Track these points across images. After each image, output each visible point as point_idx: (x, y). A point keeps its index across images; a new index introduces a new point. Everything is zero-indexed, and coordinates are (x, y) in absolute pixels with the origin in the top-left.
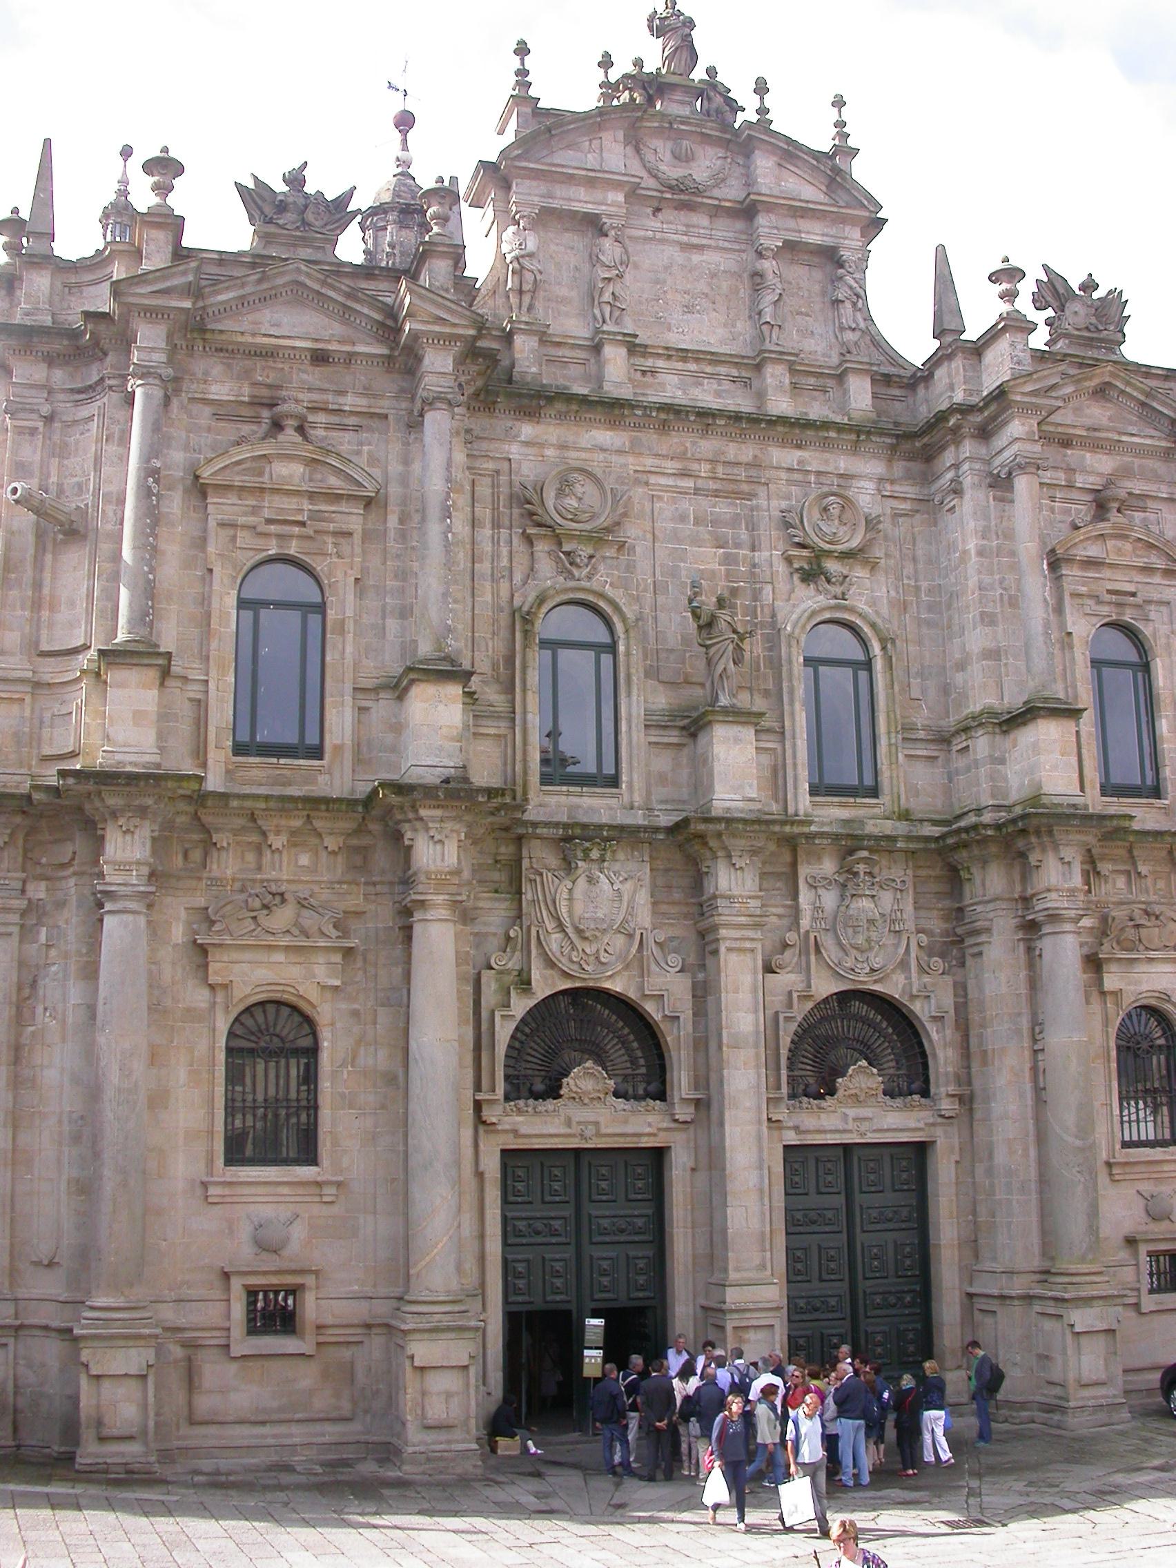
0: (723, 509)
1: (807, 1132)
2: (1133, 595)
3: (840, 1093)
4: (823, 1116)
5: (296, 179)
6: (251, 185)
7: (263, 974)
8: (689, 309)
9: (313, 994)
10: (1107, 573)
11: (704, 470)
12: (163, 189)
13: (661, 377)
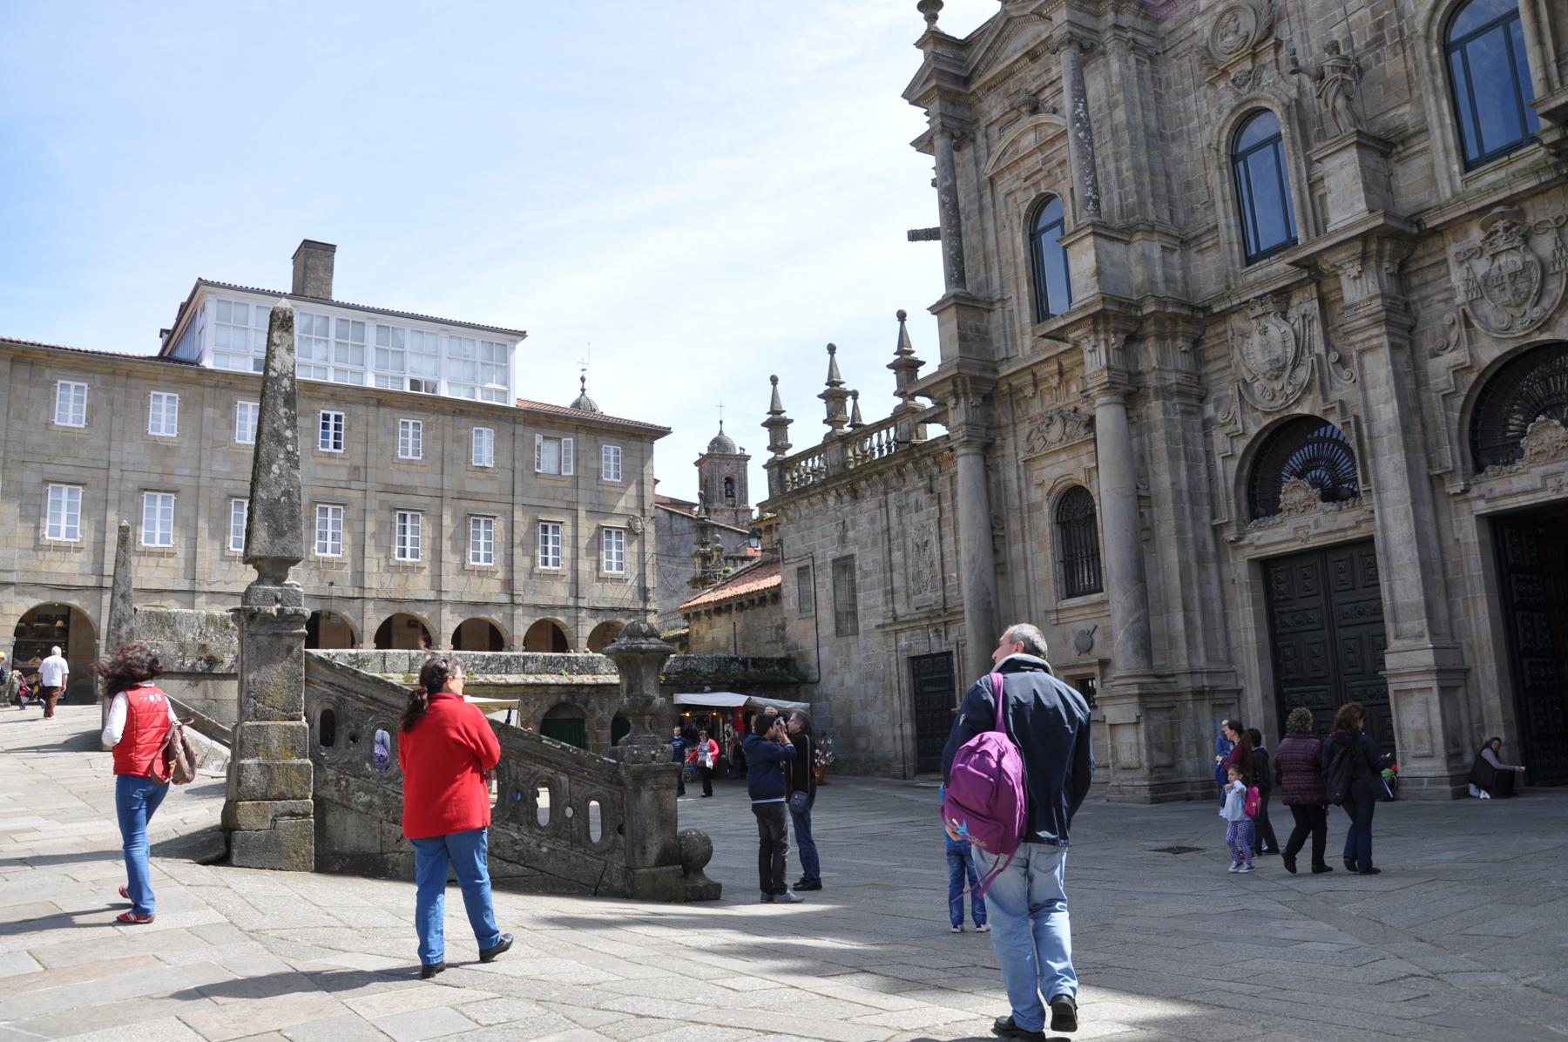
1: (1494, 499)
3: (1527, 452)
4: (1513, 479)
7: (1058, 471)
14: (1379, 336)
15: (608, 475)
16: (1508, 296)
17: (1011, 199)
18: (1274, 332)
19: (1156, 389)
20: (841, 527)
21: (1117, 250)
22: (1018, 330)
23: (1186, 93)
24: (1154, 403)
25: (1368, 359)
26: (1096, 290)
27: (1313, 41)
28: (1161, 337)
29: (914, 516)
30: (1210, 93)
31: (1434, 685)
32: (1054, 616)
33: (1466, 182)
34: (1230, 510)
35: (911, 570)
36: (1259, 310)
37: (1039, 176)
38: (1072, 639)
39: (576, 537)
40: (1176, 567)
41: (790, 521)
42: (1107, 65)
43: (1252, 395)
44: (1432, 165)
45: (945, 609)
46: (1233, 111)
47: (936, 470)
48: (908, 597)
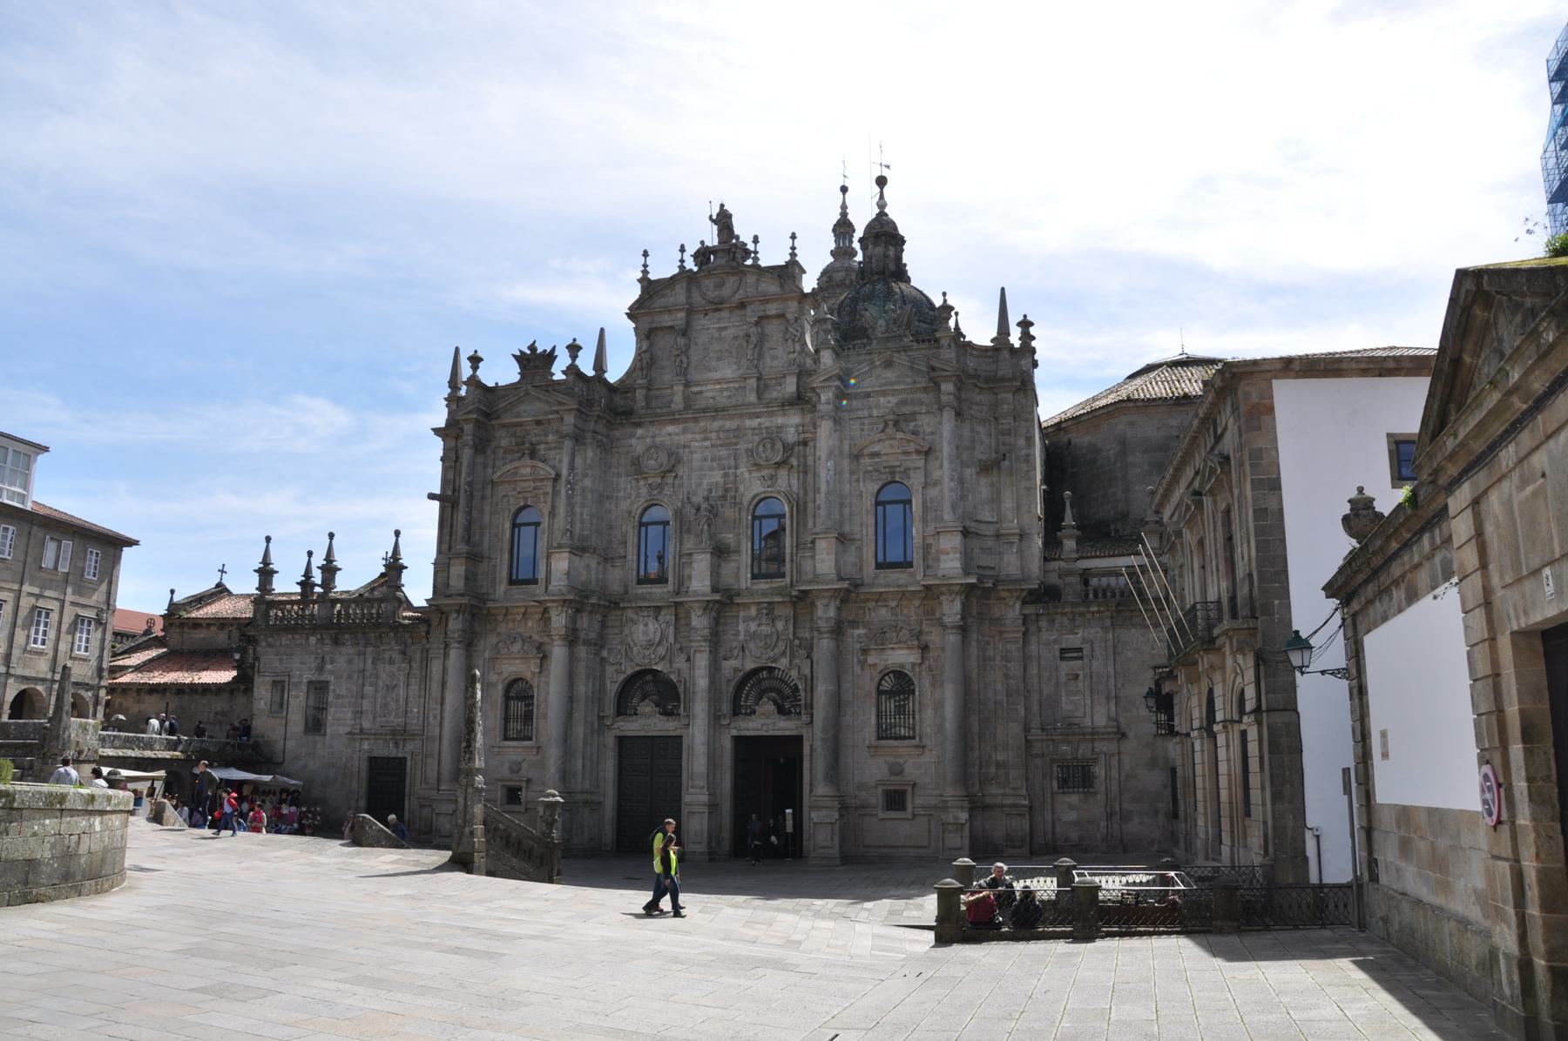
0: (723, 452)
2: (899, 466)
5: (532, 347)
6: (518, 354)
7: (513, 669)
8: (719, 359)
9: (528, 676)
10: (884, 458)
11: (714, 435)
12: (475, 368)
13: (704, 395)
14: (705, 647)
15: (89, 575)
16: (762, 644)
17: (505, 499)
18: (651, 626)
19: (584, 640)
20: (319, 661)
21: (576, 559)
22: (498, 579)
23: (619, 475)
24: (582, 647)
25: (698, 655)
26: (566, 583)
27: (693, 481)
28: (590, 613)
29: (388, 667)
30: (634, 483)
31: (706, 811)
32: (497, 750)
33: (752, 584)
34: (610, 709)
35: (379, 700)
36: (645, 613)
37: (529, 495)
38: (506, 766)
39: (60, 623)
40: (581, 736)
41: (269, 645)
42: (585, 451)
43: (632, 652)
44: (738, 568)
45: (405, 731)
46: (647, 501)
47: (410, 641)
48: (374, 718)
